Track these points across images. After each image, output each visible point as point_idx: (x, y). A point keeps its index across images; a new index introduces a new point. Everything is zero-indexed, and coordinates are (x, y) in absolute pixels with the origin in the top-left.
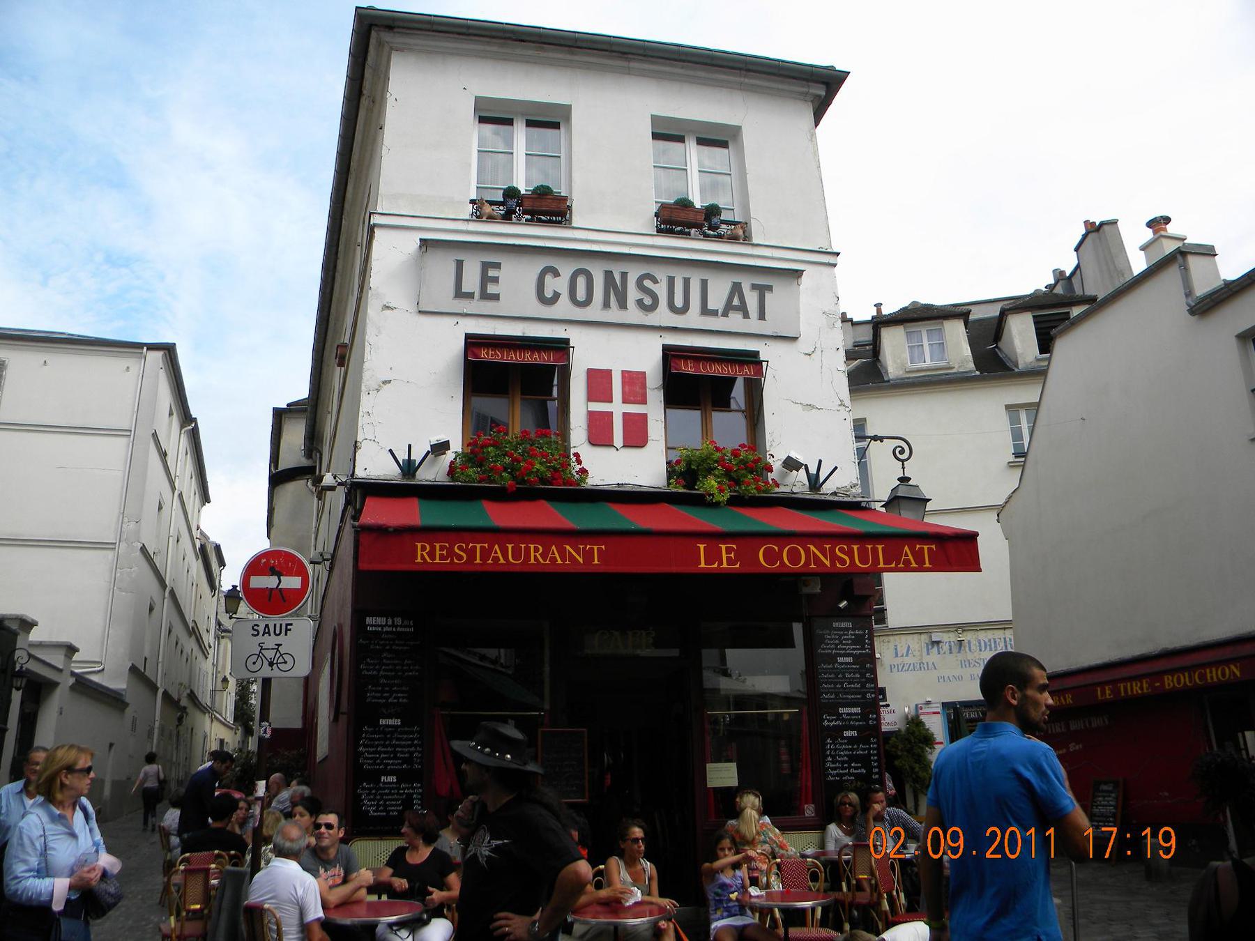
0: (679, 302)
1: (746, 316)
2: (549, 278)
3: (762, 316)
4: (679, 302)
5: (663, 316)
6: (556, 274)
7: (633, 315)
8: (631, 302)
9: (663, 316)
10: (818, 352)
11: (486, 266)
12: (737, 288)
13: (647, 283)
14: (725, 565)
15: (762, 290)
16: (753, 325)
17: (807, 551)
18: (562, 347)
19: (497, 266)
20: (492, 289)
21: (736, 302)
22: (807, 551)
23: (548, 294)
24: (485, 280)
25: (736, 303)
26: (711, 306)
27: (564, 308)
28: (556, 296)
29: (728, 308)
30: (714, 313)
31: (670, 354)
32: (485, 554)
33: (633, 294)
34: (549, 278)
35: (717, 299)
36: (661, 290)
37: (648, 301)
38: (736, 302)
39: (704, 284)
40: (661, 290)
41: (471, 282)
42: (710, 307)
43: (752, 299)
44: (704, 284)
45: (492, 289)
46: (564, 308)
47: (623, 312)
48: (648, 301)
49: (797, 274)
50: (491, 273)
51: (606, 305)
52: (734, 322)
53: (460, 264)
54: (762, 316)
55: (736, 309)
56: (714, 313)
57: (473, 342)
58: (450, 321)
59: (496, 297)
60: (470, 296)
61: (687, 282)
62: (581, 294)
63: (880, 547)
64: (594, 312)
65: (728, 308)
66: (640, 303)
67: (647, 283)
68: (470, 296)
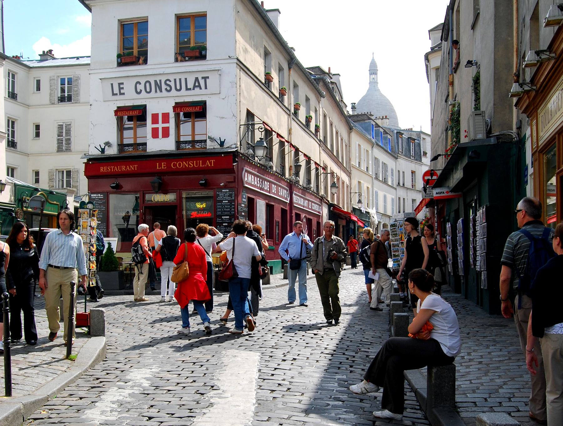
0: (178, 88)
2: (138, 85)
3: (206, 88)
4: (178, 88)
6: (139, 83)
7: (164, 93)
10: (227, 98)
11: (120, 84)
12: (197, 79)
13: (168, 82)
14: (163, 168)
15: (205, 78)
17: (183, 163)
18: (145, 107)
19: (123, 84)
20: (122, 91)
21: (197, 84)
22: (183, 163)
23: (139, 91)
24: (120, 89)
25: (197, 85)
26: (188, 87)
28: (141, 91)
30: (190, 89)
32: (114, 169)
33: (164, 87)
34: (138, 85)
35: (190, 85)
36: (172, 84)
37: (168, 89)
38: (197, 84)
39: (186, 79)
40: (172, 84)
41: (116, 90)
42: (188, 87)
44: (186, 79)
45: (122, 91)
48: (168, 89)
50: (121, 86)
51: (156, 92)
53: (112, 84)
54: (206, 88)
55: (197, 86)
56: (190, 89)
59: (124, 94)
60: (116, 94)
61: (180, 80)
62: (148, 90)
63: (201, 161)
64: (153, 94)
65: (195, 86)
66: (166, 89)
67: (168, 82)
68: (116, 94)
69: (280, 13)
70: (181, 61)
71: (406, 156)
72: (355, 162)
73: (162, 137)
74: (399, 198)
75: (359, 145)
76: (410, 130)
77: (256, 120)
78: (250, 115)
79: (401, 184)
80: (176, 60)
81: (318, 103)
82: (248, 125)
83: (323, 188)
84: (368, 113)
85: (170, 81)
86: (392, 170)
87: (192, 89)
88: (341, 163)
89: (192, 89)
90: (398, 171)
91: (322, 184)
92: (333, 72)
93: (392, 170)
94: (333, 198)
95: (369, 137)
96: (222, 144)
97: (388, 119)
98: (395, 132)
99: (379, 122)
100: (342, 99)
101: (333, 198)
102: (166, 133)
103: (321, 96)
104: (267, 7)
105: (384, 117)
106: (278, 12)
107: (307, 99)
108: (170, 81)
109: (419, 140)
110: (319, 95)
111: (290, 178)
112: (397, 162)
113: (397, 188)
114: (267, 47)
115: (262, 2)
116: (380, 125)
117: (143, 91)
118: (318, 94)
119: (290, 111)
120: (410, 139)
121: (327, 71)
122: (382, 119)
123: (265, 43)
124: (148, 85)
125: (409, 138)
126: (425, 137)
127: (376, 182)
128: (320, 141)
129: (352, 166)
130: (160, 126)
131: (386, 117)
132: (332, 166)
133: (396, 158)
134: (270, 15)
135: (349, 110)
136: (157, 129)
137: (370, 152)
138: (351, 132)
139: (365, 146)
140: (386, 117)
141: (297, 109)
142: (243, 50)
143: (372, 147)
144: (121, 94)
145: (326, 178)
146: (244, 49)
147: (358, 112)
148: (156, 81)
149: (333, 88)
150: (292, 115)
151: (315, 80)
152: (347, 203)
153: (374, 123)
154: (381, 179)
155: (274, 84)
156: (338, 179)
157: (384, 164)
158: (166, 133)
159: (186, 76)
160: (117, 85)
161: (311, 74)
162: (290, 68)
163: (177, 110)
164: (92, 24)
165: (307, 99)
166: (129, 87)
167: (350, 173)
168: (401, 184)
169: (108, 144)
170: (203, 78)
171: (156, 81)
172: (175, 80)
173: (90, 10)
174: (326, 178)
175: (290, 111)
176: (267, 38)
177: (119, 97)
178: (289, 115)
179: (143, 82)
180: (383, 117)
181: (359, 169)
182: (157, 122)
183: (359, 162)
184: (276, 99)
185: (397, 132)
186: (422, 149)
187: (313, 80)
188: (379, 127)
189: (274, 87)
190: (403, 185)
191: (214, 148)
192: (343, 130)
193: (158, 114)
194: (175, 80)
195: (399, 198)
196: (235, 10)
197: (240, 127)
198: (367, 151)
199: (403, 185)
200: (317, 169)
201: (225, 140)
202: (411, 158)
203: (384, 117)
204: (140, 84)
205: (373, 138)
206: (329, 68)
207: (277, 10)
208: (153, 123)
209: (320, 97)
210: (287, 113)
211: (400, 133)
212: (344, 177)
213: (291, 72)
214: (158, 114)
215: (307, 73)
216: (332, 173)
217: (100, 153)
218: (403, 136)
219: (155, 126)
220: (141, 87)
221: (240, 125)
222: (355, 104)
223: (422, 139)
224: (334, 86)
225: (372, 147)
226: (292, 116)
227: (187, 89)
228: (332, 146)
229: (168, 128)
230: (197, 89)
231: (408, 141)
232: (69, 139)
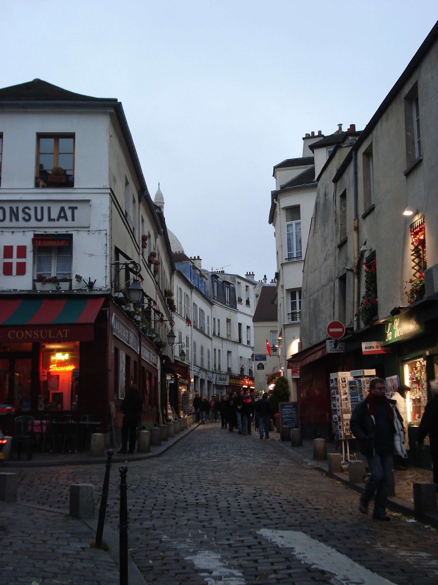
0: (39, 217)
1: (67, 220)
3: (73, 219)
4: (39, 217)
5: (33, 223)
7: (22, 223)
9: (33, 223)
12: (62, 209)
13: (27, 210)
15: (73, 209)
16: (70, 223)
21: (62, 215)
25: (62, 215)
29: (59, 217)
30: (54, 220)
35: (54, 215)
36: (32, 213)
37: (27, 217)
38: (62, 215)
39: (49, 209)
40: (32, 213)
43: (69, 213)
44: (49, 209)
47: (17, 223)
48: (27, 217)
49: (88, 201)
51: (11, 220)
52: (62, 222)
54: (73, 219)
55: (63, 217)
56: (54, 220)
61: (42, 208)
65: (59, 217)
66: (24, 219)
67: (27, 210)
70: (43, 187)
80: (37, 185)
85: (29, 209)
87: (56, 219)
89: (56, 219)
102: (21, 269)
108: (29, 209)
130: (15, 260)
148: (11, 208)
163: (38, 243)
170: (70, 208)
172: (36, 209)
182: (11, 257)
194: (36, 209)
227: (50, 219)
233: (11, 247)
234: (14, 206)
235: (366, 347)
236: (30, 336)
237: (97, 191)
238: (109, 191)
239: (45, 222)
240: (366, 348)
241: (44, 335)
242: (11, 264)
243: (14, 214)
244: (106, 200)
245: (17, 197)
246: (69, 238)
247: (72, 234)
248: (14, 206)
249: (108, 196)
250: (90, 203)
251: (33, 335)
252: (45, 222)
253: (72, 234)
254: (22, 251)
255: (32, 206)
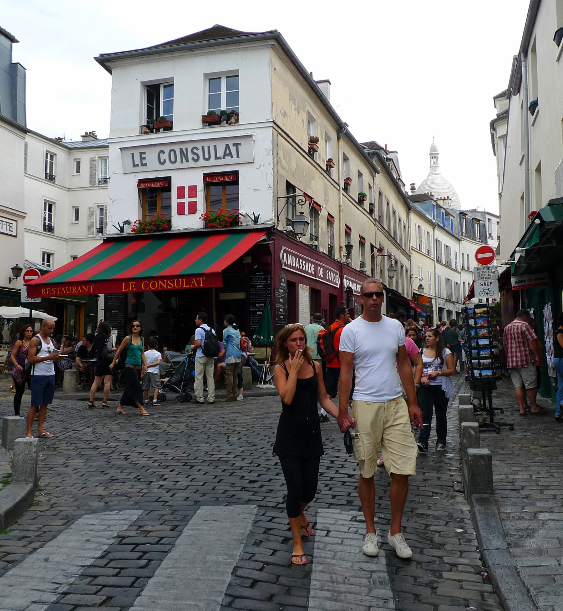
0: (207, 156)
1: (232, 157)
2: (161, 154)
3: (238, 156)
4: (207, 156)
5: (202, 162)
7: (191, 164)
8: (190, 159)
9: (202, 162)
11: (141, 154)
12: (227, 146)
13: (195, 151)
15: (237, 145)
19: (144, 153)
21: (228, 152)
23: (162, 161)
24: (142, 159)
25: (228, 153)
27: (168, 165)
28: (165, 160)
30: (220, 158)
31: (206, 176)
33: (190, 156)
35: (220, 153)
36: (200, 152)
37: (196, 158)
38: (228, 152)
39: (215, 146)
40: (200, 152)
41: (137, 161)
44: (215, 146)
45: (144, 162)
46: (168, 165)
47: (188, 163)
48: (196, 158)
49: (251, 136)
50: (143, 156)
51: (182, 161)
52: (228, 160)
53: (133, 154)
54: (238, 156)
55: (228, 155)
56: (220, 158)
57: (141, 182)
58: (133, 175)
59: (146, 165)
60: (138, 165)
61: (209, 147)
62: (173, 160)
64: (178, 165)
65: (225, 155)
66: (193, 158)
67: (195, 151)
68: (138, 165)
69: (330, 84)
71: (470, 238)
72: (414, 244)
73: (189, 214)
74: (464, 283)
75: (419, 226)
76: (474, 211)
77: (298, 192)
78: (290, 187)
79: (466, 268)
81: (372, 179)
82: (288, 197)
83: (379, 271)
84: (428, 193)
85: (198, 149)
86: (456, 253)
87: (222, 158)
88: (399, 244)
89: (222, 158)
90: (463, 254)
91: (378, 267)
92: (389, 149)
93: (456, 253)
94: (390, 283)
95: (430, 218)
96: (256, 220)
97: (450, 199)
98: (458, 212)
99: (441, 203)
100: (399, 177)
101: (390, 283)
102: (193, 209)
103: (377, 172)
104: (316, 78)
105: (446, 198)
106: (328, 83)
107: (360, 175)
108: (198, 149)
109: (484, 221)
110: (373, 171)
111: (340, 260)
112: (461, 244)
113: (461, 272)
114: (311, 112)
115: (311, 73)
116: (442, 206)
117: (168, 161)
118: (372, 169)
119: (339, 186)
120: (474, 220)
121: (384, 147)
122: (443, 200)
123: (308, 108)
124: (172, 154)
125: (473, 219)
126: (490, 217)
127: (438, 265)
128: (375, 220)
129: (412, 249)
130: (187, 200)
131: (448, 197)
132: (389, 248)
133: (460, 241)
134: (320, 86)
135: (407, 190)
136: (183, 204)
137: (431, 233)
138: (410, 212)
139: (426, 227)
140: (448, 197)
141: (347, 182)
142: (282, 114)
143: (434, 229)
144: (143, 165)
145: (382, 261)
146: (283, 112)
147: (417, 192)
148: (181, 150)
149: (389, 164)
150: (341, 189)
151: (369, 154)
152: (407, 289)
153: (435, 204)
154: (444, 263)
155: (319, 155)
156: (396, 262)
157: (447, 246)
158: (193, 209)
159: (215, 143)
160: (139, 155)
161: (364, 148)
162: (339, 139)
164: (112, 88)
165: (360, 175)
166: (151, 157)
167: (410, 256)
168: (466, 268)
169: (127, 222)
170: (234, 145)
171: (181, 150)
172: (203, 148)
173: (110, 72)
174: (382, 261)
175: (339, 186)
176: (312, 103)
177: (140, 169)
178: (339, 190)
179: (167, 149)
180: (444, 198)
181: (419, 251)
182: (183, 197)
183: (420, 245)
184: (322, 172)
185: (460, 213)
186: (487, 230)
187: (367, 156)
188: (441, 207)
189: (319, 158)
190: (468, 268)
191: (247, 225)
192: (401, 210)
193: (184, 187)
194: (203, 148)
195: (464, 283)
196: (270, 67)
197: (278, 200)
198: (428, 233)
199: (468, 268)
200: (372, 251)
201: (259, 215)
202: (476, 241)
203: (446, 198)
204: (164, 153)
205: (434, 219)
206: (386, 146)
207: (328, 81)
208: (178, 198)
209: (374, 173)
210: (336, 188)
211: (463, 214)
212: (402, 259)
213: (340, 143)
214: (184, 187)
215: (360, 148)
216: (390, 256)
217: (119, 232)
218: (467, 216)
219: (181, 201)
220: (165, 157)
221: (278, 198)
222: (414, 184)
223: (487, 219)
224: (391, 163)
225: (434, 229)
226: (342, 191)
227: (217, 158)
228: (389, 226)
229: (179, 197)
230: (228, 158)
231: (473, 222)
232: (90, 219)
233: (183, 188)
234: (183, 147)
235: (516, 281)
236: (165, 287)
237: (261, 125)
238: (272, 124)
239: (213, 161)
240: (516, 282)
241: (178, 285)
242: (183, 204)
243: (184, 155)
244: (269, 133)
245: (188, 139)
246: (235, 174)
247: (237, 171)
248: (183, 147)
249: (272, 128)
250: (253, 138)
251: (167, 284)
252: (213, 161)
253: (237, 171)
254: (193, 190)
255: (199, 146)
